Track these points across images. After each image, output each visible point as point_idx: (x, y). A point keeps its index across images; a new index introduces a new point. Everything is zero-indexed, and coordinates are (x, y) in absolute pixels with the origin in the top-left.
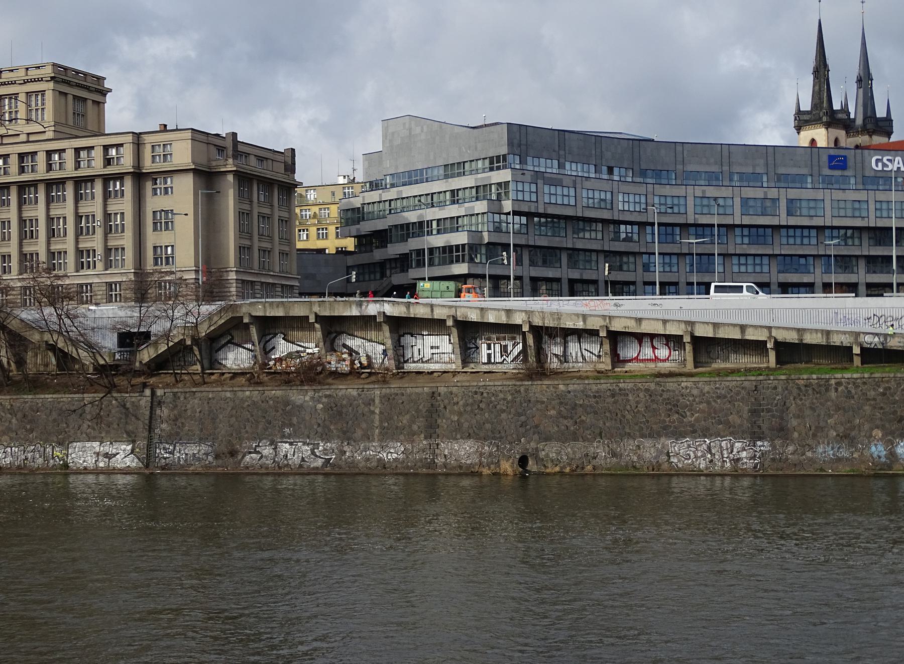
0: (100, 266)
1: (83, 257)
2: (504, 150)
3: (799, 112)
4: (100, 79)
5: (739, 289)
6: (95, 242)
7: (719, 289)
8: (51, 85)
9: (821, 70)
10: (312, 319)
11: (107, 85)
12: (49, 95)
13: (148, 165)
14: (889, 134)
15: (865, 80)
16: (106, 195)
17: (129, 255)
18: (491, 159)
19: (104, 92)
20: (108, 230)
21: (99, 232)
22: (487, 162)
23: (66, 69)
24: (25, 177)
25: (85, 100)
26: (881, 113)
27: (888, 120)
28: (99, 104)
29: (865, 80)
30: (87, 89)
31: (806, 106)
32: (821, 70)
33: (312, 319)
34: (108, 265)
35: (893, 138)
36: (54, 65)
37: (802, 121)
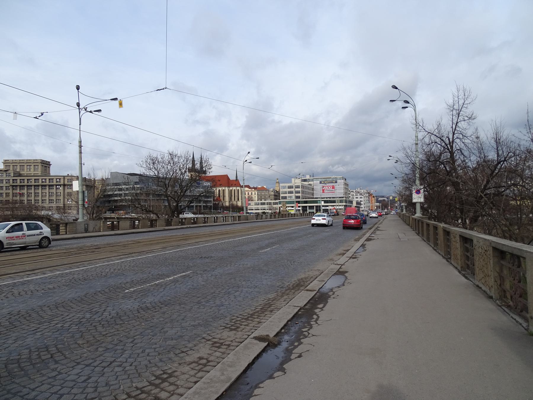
0: (55, 203)
1: (51, 201)
2: (138, 181)
4: (49, 162)
5: (189, 214)
6: (54, 198)
7: (186, 214)
8: (40, 164)
10: (116, 218)
11: (51, 163)
12: (40, 166)
13: (66, 183)
14: (206, 174)
15: (201, 163)
16: (57, 189)
17: (62, 201)
18: (135, 182)
19: (50, 165)
20: (57, 196)
21: (55, 196)
22: (134, 183)
23: (43, 160)
24: (36, 184)
25: (46, 167)
28: (49, 167)
30: (47, 164)
33: (116, 218)
34: (57, 203)
36: (41, 160)
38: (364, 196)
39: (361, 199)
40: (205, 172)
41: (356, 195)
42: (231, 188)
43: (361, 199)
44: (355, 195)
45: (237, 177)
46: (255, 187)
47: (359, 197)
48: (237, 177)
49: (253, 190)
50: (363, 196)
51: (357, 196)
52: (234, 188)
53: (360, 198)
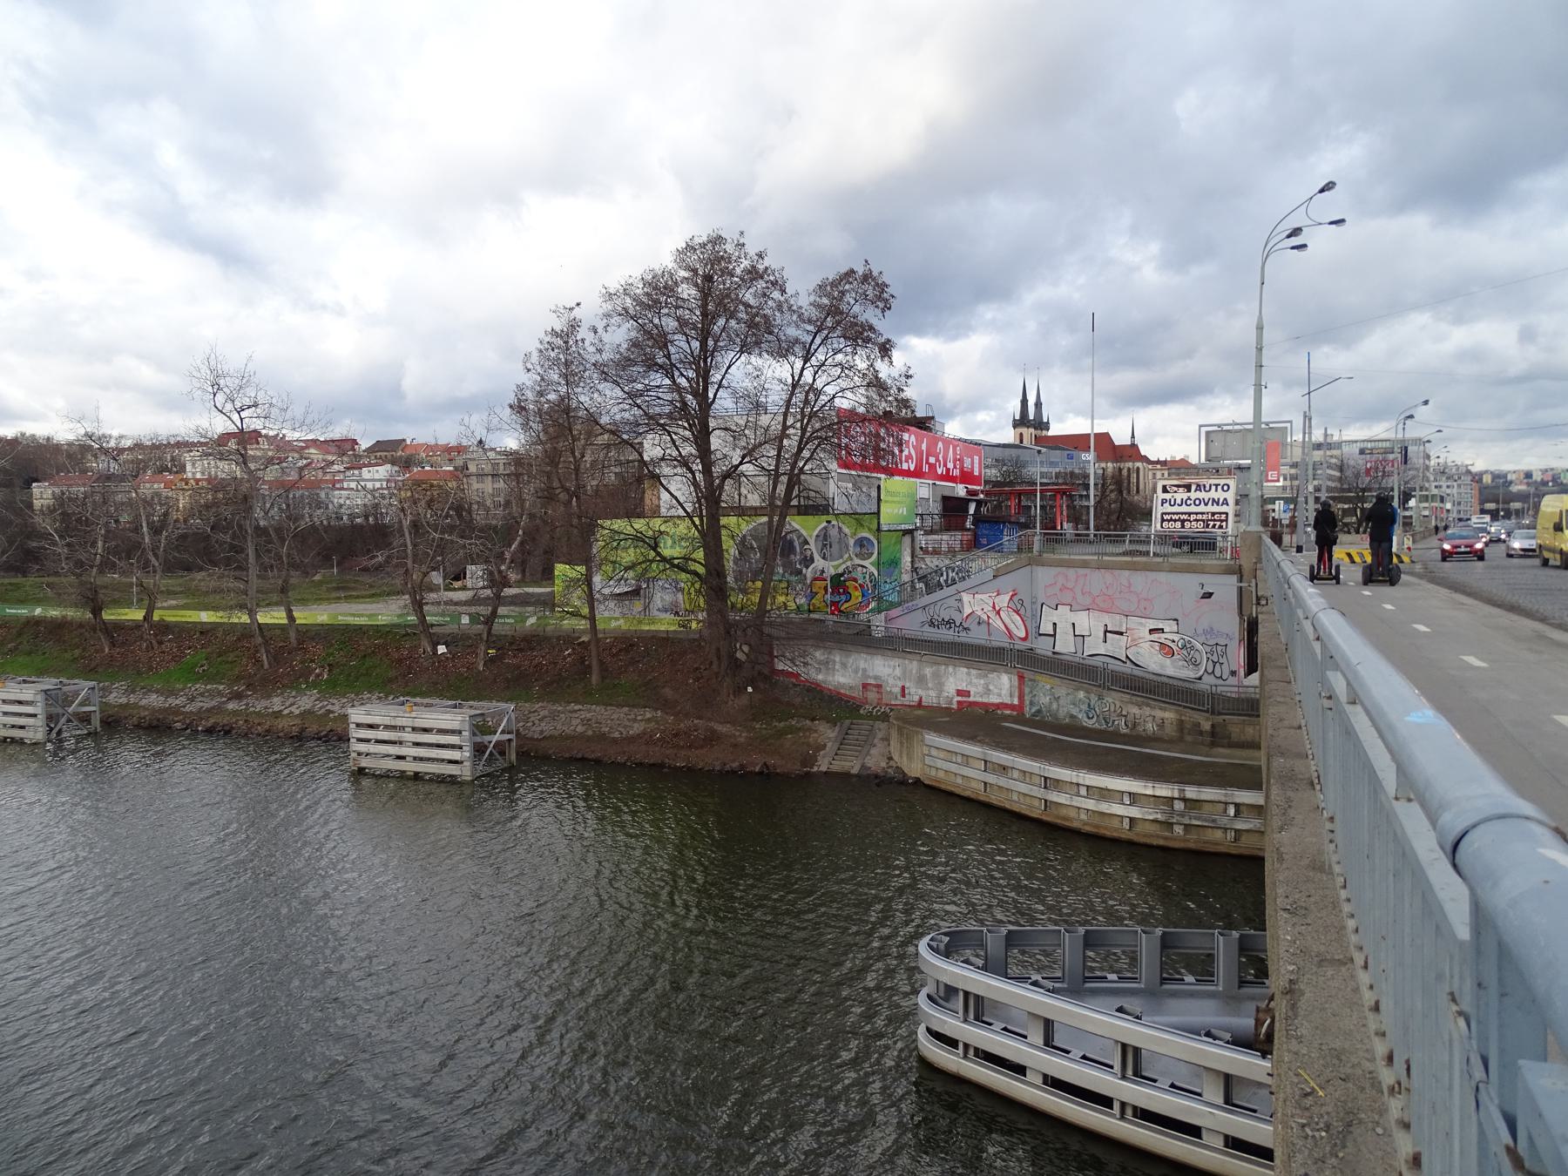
3: (1014, 420)
9: (1024, 402)
15: (1038, 405)
26: (1045, 420)
27: (1048, 423)
29: (1038, 405)
31: (1017, 417)
32: (1024, 402)
35: (1050, 433)
37: (1016, 424)
38: (1459, 482)
39: (1448, 491)
40: (1046, 426)
41: (1436, 480)
42: (1122, 465)
43: (1448, 491)
44: (1432, 478)
45: (1133, 436)
46: (1162, 459)
47: (1444, 485)
48: (1133, 436)
49: (1159, 467)
50: (1455, 484)
51: (1436, 484)
52: (1130, 465)
53: (1448, 487)
